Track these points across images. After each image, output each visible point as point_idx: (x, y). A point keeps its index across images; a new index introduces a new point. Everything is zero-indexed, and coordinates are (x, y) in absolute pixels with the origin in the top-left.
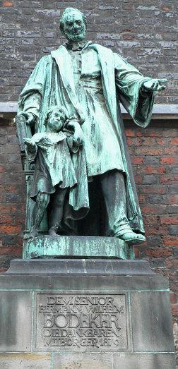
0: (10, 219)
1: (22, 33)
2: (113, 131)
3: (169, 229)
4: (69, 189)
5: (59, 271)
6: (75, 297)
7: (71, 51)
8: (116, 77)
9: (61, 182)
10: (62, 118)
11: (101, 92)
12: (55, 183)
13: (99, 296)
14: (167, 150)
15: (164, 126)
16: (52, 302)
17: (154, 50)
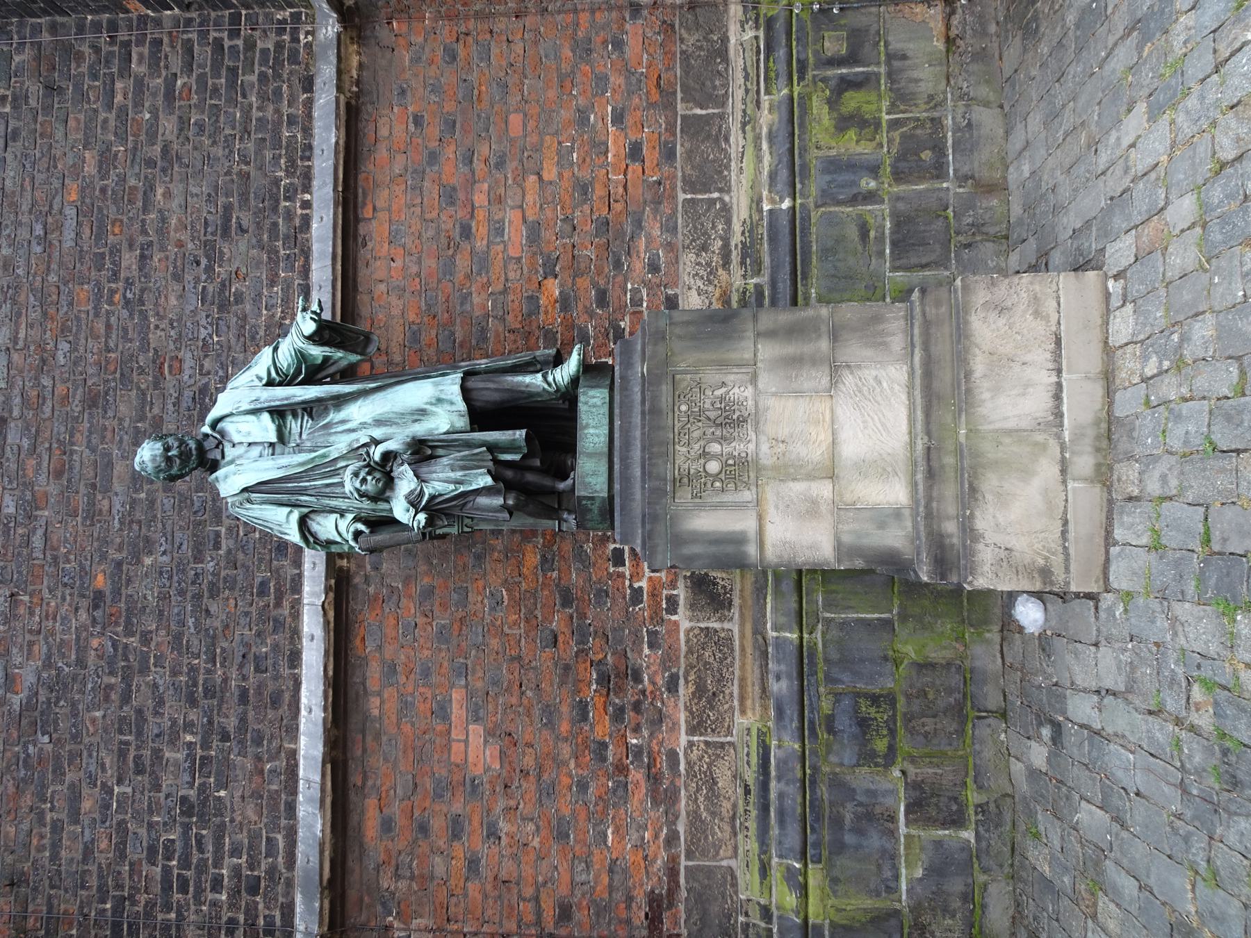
0: (513, 561)
1: (164, 553)
2: (390, 390)
3: (529, 315)
4: (496, 461)
5: (637, 472)
6: (677, 447)
7: (223, 462)
8: (280, 384)
9: (489, 472)
10: (369, 473)
11: (310, 409)
12: (488, 481)
13: (677, 413)
14: (396, 312)
16: (685, 480)
17: (203, 322)
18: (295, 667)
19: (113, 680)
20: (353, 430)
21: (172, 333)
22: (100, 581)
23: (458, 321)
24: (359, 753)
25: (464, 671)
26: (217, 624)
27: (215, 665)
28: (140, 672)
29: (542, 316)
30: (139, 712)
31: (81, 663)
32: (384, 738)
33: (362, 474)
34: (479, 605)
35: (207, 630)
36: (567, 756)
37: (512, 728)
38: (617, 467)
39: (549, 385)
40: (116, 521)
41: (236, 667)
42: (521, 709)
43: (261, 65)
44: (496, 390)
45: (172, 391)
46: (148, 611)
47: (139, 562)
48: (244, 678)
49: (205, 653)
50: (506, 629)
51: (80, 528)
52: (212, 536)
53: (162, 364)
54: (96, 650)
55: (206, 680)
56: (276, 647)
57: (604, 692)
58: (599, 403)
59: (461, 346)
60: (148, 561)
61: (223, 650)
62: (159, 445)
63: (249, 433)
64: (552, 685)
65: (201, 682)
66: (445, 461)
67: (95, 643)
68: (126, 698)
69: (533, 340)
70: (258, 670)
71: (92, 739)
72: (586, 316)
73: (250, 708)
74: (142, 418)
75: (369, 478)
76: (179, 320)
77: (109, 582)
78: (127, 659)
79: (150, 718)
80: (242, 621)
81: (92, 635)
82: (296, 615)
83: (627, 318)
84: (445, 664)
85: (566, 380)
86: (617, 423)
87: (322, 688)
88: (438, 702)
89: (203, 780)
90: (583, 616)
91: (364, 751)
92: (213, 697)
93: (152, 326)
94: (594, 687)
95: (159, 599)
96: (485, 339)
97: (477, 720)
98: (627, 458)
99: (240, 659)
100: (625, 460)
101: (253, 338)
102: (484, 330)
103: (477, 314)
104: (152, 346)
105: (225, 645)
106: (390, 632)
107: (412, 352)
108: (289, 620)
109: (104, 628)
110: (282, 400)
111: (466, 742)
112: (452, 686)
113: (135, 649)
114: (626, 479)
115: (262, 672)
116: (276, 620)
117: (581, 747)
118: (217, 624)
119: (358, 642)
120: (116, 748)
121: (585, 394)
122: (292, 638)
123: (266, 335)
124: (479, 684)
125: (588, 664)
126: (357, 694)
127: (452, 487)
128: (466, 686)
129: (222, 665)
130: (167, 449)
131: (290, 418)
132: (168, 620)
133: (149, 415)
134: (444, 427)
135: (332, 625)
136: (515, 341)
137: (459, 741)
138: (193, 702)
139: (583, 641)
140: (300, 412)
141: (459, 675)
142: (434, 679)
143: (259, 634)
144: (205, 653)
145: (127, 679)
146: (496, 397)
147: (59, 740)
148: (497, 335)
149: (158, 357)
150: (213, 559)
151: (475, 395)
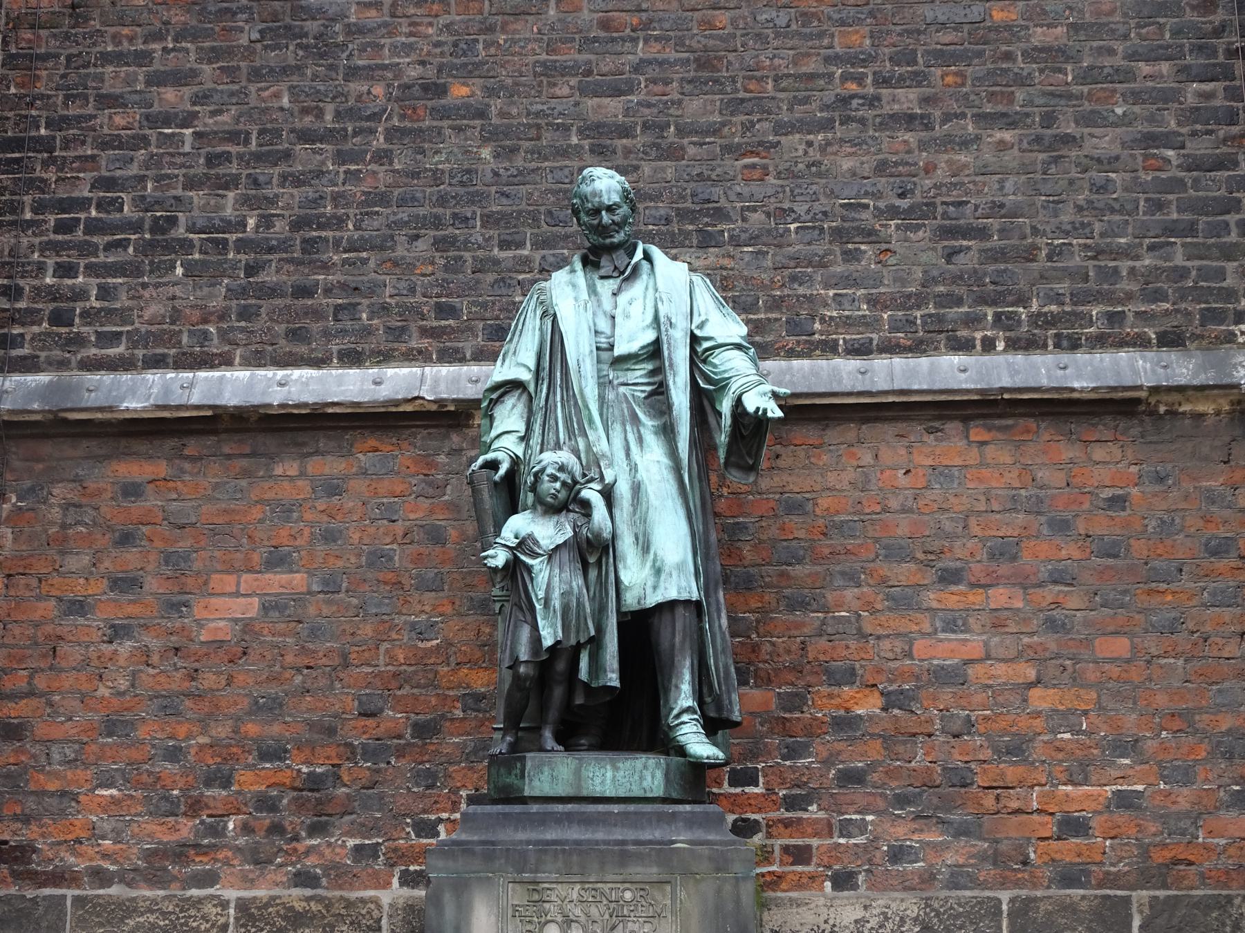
0: (478, 654)
1: (496, 174)
2: (678, 502)
3: (827, 672)
4: (578, 647)
5: (550, 835)
6: (578, 887)
7: (596, 276)
8: (693, 351)
9: (558, 643)
10: (564, 484)
11: (659, 394)
12: (548, 642)
13: (621, 887)
14: (832, 478)
15: (827, 418)
16: (536, 897)
18: (340, 359)
19: (329, 117)
20: (628, 454)
22: (459, 91)
23: (818, 568)
24: (226, 450)
25: (330, 587)
26: (400, 252)
27: (345, 251)
29: (825, 689)
30: (287, 155)
31: (353, 73)
32: (244, 483)
33: (562, 476)
34: (419, 607)
35: (392, 237)
36: (213, 733)
37: (253, 655)
38: (560, 808)
39: (678, 716)
40: (540, 107)
41: (342, 278)
42: (277, 668)
43: (1199, 269)
44: (673, 646)
46: (419, 157)
47: (485, 141)
48: (328, 291)
49: (362, 238)
50: (385, 645)
51: (531, 59)
52: (517, 237)
53: (758, 154)
54: (369, 93)
55: (326, 240)
56: (368, 332)
57: (298, 784)
58: (645, 784)
59: (782, 574)
60: (486, 153)
61: (365, 262)
62: (616, 198)
63: (628, 317)
64: (308, 710)
65: (324, 234)
66: (577, 583)
67: (378, 90)
68: (305, 136)
70: (338, 309)
71: (253, 95)
72: (825, 754)
73: (288, 301)
74: (681, 132)
75: (558, 485)
77: (458, 102)
78: (355, 134)
79: (277, 170)
80: (403, 285)
81: (389, 86)
82: (411, 357)
83: (822, 815)
84: (340, 563)
85: (681, 739)
86: (616, 808)
87: (311, 400)
88: (290, 554)
89: (197, 244)
90: (400, 753)
91: (229, 457)
92: (304, 251)
93: (811, 137)
94: (305, 770)
95: (435, 171)
96: (791, 608)
97: (265, 608)
98: (570, 822)
99: (353, 285)
100: (569, 818)
101: (793, 279)
102: (804, 605)
104: (783, 139)
105: (372, 264)
106: (385, 486)
107: (772, 504)
108: (403, 347)
109: (398, 100)
110: (670, 359)
111: (237, 594)
112: (311, 574)
114: (543, 821)
115: (335, 315)
116: (403, 330)
117: (225, 751)
118: (400, 252)
119: (372, 442)
120: (241, 127)
121: (658, 765)
122: (379, 353)
123: (798, 296)
124: (312, 610)
125: (336, 761)
126: (304, 444)
127: (541, 594)
128: (310, 593)
129: (345, 261)
130: (610, 209)
131: (650, 366)
132: (406, 185)
133: (686, 141)
134: (626, 577)
135: (394, 409)
136: (789, 652)
137: (238, 584)
138: (297, 225)
139: (369, 753)
140: (656, 379)
141: (325, 582)
142: (320, 548)
143: (385, 308)
144: (362, 236)
145: (328, 136)
146: (665, 644)
147: (254, 52)
149: (768, 148)
150: (486, 240)
151: (666, 617)
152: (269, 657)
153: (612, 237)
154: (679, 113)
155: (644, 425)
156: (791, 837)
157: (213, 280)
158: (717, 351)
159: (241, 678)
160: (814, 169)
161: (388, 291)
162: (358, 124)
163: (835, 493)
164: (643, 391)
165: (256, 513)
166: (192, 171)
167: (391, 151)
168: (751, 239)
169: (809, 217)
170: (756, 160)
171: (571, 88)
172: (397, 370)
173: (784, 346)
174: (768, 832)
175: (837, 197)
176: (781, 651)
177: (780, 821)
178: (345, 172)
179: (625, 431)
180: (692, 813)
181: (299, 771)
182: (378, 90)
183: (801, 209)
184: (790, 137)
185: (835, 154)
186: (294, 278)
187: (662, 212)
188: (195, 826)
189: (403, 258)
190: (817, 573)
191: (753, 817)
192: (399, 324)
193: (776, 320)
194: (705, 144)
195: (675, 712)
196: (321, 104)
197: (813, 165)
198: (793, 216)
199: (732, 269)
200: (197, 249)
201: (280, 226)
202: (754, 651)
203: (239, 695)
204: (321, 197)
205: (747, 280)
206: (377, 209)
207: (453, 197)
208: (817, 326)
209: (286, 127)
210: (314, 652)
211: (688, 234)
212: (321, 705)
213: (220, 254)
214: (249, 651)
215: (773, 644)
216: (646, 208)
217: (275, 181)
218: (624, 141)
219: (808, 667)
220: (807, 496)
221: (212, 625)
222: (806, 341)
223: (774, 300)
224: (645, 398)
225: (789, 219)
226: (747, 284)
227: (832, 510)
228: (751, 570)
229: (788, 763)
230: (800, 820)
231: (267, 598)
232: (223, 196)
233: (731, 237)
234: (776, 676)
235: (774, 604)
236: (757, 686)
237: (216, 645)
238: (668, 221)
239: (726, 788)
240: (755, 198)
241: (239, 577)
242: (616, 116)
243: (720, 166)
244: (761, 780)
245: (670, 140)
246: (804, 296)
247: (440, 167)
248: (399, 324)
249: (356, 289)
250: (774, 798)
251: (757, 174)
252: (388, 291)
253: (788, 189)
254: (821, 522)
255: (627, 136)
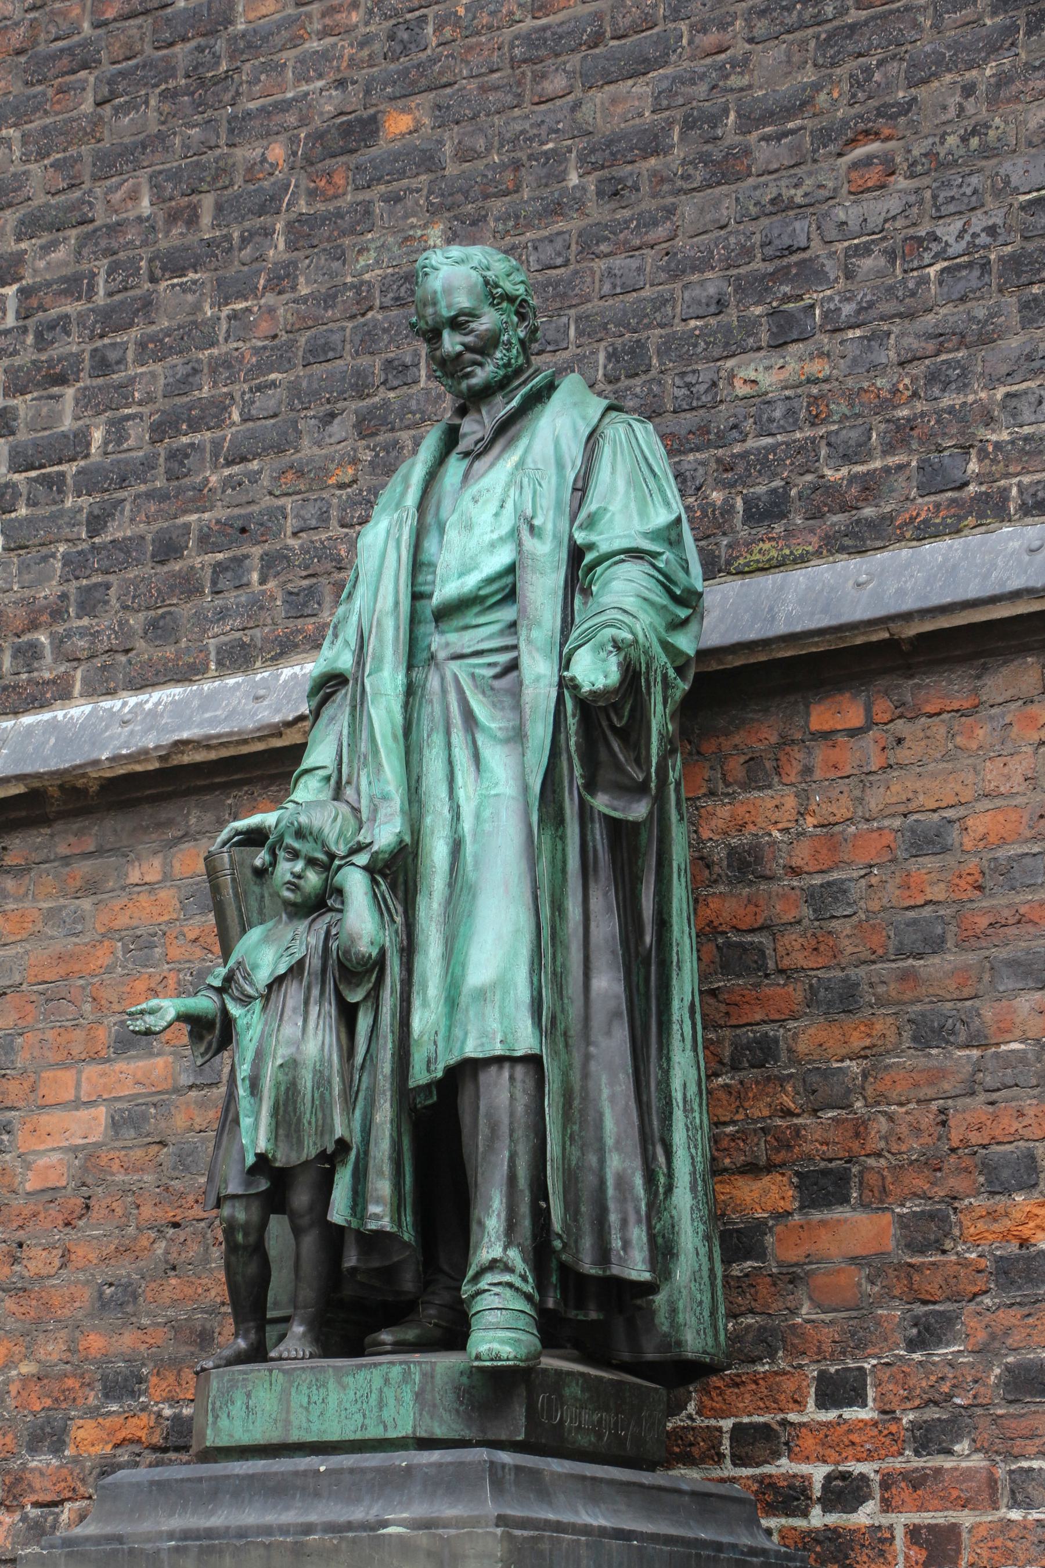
3: (988, 1168)
5: (218, 1519)
14: (992, 774)
17: (978, 222)
21: (952, 140)
23: (971, 958)
24: (62, 850)
26: (307, 450)
27: (229, 463)
28: (220, 283)
29: (980, 1203)
32: (86, 904)
36: (41, 1354)
37: (98, 1212)
42: (131, 1230)
45: (809, 183)
46: (336, 265)
47: (433, 212)
51: (508, 33)
54: (264, 159)
56: (258, 605)
57: (157, 1439)
58: (386, 1415)
59: (906, 976)
61: (254, 477)
62: (463, 301)
65: (197, 438)
67: (277, 152)
69: (920, 1183)
70: (219, 568)
71: (100, 207)
72: (981, 1336)
74: (748, 122)
76: (987, 152)
77: (397, 145)
78: (244, 241)
83: (978, 1461)
89: (23, 489)
91: (66, 860)
97: (115, 1125)
99: (239, 524)
103: (988, 1014)
104: (922, 93)
105: (265, 481)
107: (888, 838)
111: (77, 1104)
113: (261, 258)
115: (214, 583)
117: (55, 1386)
118: (307, 450)
120: (85, 267)
123: (939, 413)
124: (180, 1121)
126: (169, 823)
129: (228, 483)
130: (456, 324)
133: (755, 135)
137: (78, 1085)
138: (159, 431)
148: (936, 1075)
149: (893, 117)
152: (119, 1211)
153: (468, 376)
154: (745, 81)
155: (484, 729)
156: (920, 1509)
157: (44, 550)
158: (599, 570)
159: (81, 1252)
160: (974, 142)
161: (290, 524)
162: (247, 224)
163: (999, 802)
164: (490, 665)
165: (102, 957)
166: (17, 361)
167: (294, 263)
168: (858, 312)
169: (963, 244)
170: (874, 147)
171: (570, 75)
172: (297, 669)
173: (912, 519)
174: (883, 1500)
175: (1016, 191)
176: (903, 1130)
177: (905, 1475)
178: (229, 318)
179: (449, 745)
180: (439, 1465)
181: (159, 1415)
182: (277, 152)
183: (949, 231)
184: (936, 84)
185: (1017, 99)
186: (155, 527)
187: (712, 290)
188: (14, 1524)
189: (311, 460)
190: (967, 968)
191: (858, 1468)
192: (306, 583)
193: (900, 467)
194: (786, 134)
195: (471, 1273)
196: (195, 198)
197: (974, 132)
198: (935, 247)
199: (826, 380)
200: (22, 502)
201: (137, 434)
202: (857, 1135)
203: (77, 1282)
204: (195, 371)
205: (851, 396)
206: (272, 376)
207: (385, 331)
208: (973, 466)
209: (146, 253)
210: (182, 1195)
211: (749, 326)
212: (189, 1291)
213: (55, 503)
214: (92, 1202)
215: (890, 1118)
216: (685, 287)
217: (130, 355)
218: (653, 161)
219: (953, 1159)
220: (949, 814)
221: (43, 1161)
222: (953, 501)
223: (898, 429)
224: (496, 677)
225: (927, 257)
226: (852, 406)
227: (992, 838)
228: (852, 972)
229: (917, 1356)
230: (938, 1471)
231: (119, 1105)
232: (57, 398)
233: (825, 315)
234: (896, 1181)
235: (893, 1038)
236: (864, 1206)
237: (47, 1197)
238: (721, 304)
239: (812, 1413)
240: (870, 226)
241: (80, 1072)
242: (641, 115)
243: (810, 174)
244: (871, 1393)
245: (728, 142)
246: (951, 410)
247: (367, 277)
248: (306, 583)
249: (243, 530)
250: (893, 1428)
251: (873, 175)
252: (290, 524)
253: (928, 194)
254: (972, 864)
255: (656, 153)
